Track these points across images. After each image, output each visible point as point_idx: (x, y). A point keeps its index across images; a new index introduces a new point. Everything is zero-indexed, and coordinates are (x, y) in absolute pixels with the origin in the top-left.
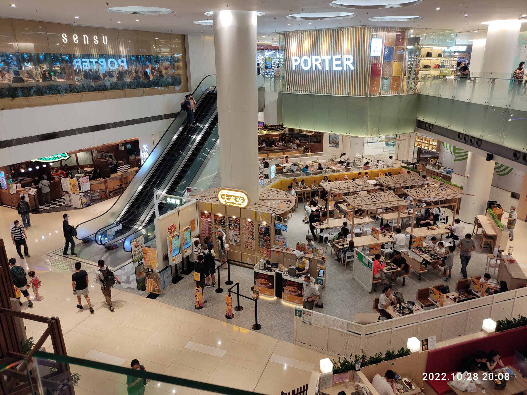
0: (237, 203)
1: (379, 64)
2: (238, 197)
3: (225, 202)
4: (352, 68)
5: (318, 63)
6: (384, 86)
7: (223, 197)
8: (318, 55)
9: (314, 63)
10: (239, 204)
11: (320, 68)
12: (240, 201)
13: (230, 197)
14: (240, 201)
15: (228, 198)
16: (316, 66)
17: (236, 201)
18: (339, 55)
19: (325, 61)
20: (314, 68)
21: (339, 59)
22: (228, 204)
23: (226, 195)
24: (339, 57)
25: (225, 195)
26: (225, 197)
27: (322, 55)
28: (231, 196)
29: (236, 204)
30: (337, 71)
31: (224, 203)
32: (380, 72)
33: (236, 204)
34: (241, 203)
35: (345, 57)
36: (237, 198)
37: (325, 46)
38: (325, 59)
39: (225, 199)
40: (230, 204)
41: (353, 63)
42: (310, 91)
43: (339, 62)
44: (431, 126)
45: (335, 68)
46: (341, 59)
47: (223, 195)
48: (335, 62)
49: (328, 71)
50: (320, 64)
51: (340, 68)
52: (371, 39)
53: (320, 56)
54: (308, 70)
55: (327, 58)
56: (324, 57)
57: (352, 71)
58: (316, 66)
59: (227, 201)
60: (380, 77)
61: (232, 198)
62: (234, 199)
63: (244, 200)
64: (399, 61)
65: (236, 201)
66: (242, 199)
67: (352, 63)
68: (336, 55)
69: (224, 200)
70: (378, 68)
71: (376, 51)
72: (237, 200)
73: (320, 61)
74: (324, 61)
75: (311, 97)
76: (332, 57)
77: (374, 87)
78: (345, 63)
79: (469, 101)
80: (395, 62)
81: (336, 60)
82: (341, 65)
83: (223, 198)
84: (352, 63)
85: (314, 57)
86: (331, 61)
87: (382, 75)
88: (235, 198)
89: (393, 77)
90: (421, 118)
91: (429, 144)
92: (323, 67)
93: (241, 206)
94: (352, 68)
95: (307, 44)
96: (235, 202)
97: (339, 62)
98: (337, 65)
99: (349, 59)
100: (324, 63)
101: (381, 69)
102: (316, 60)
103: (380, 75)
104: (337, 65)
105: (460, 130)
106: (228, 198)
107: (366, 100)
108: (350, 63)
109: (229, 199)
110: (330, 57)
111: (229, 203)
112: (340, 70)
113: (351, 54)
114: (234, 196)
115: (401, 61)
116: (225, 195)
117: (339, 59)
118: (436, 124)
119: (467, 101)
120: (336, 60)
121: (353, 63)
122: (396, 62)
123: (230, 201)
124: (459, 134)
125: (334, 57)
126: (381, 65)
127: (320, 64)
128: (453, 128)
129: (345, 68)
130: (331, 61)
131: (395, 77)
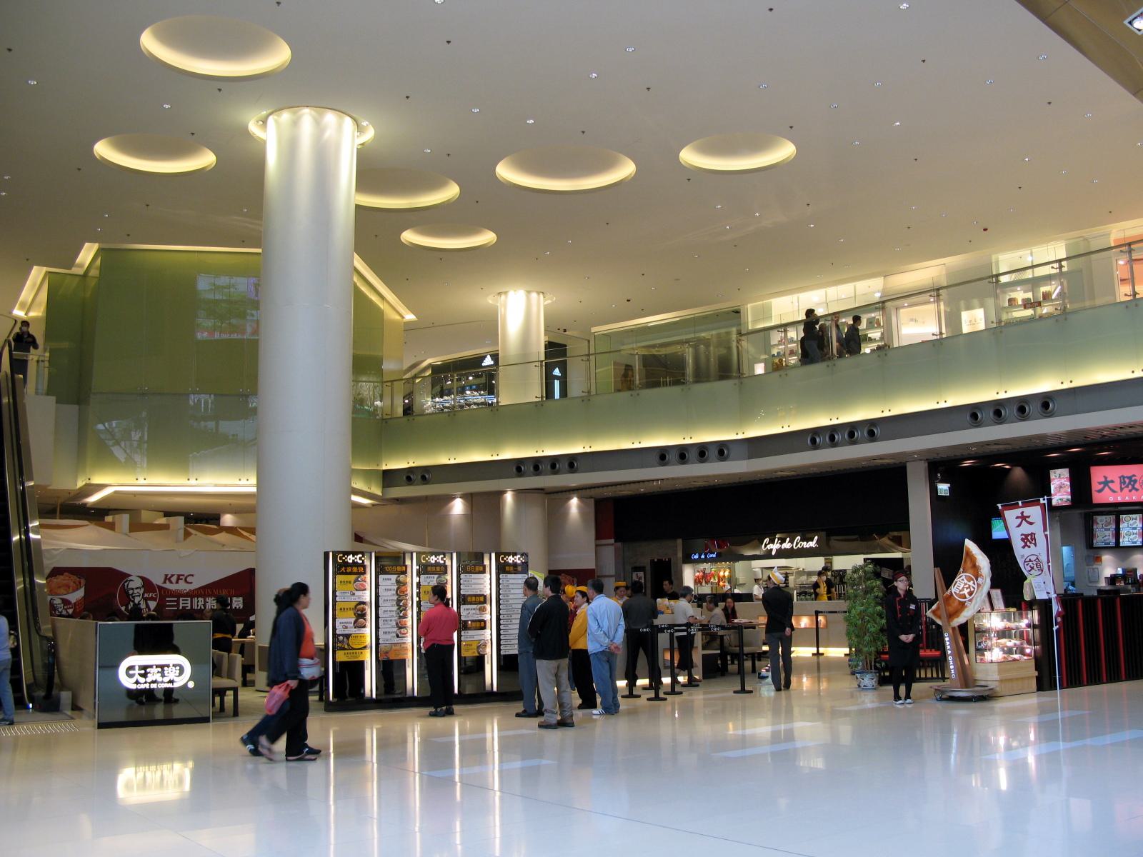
0: (166, 679)
2: (168, 666)
3: (137, 682)
7: (131, 672)
10: (171, 682)
12: (171, 674)
13: (148, 670)
14: (171, 674)
15: (143, 672)
17: (163, 676)
22: (142, 687)
23: (139, 666)
25: (137, 668)
26: (137, 671)
28: (151, 666)
29: (162, 682)
31: (134, 687)
33: (162, 682)
34: (176, 679)
36: (166, 668)
39: (137, 677)
40: (147, 686)
47: (131, 668)
59: (142, 680)
61: (154, 670)
62: (158, 672)
63: (182, 671)
65: (163, 676)
66: (178, 668)
69: (134, 680)
72: (166, 672)
83: (131, 676)
88: (160, 670)
93: (176, 685)
96: (160, 679)
106: (143, 672)
109: (145, 675)
111: (146, 683)
114: (157, 666)
116: (137, 668)
123: (149, 679)
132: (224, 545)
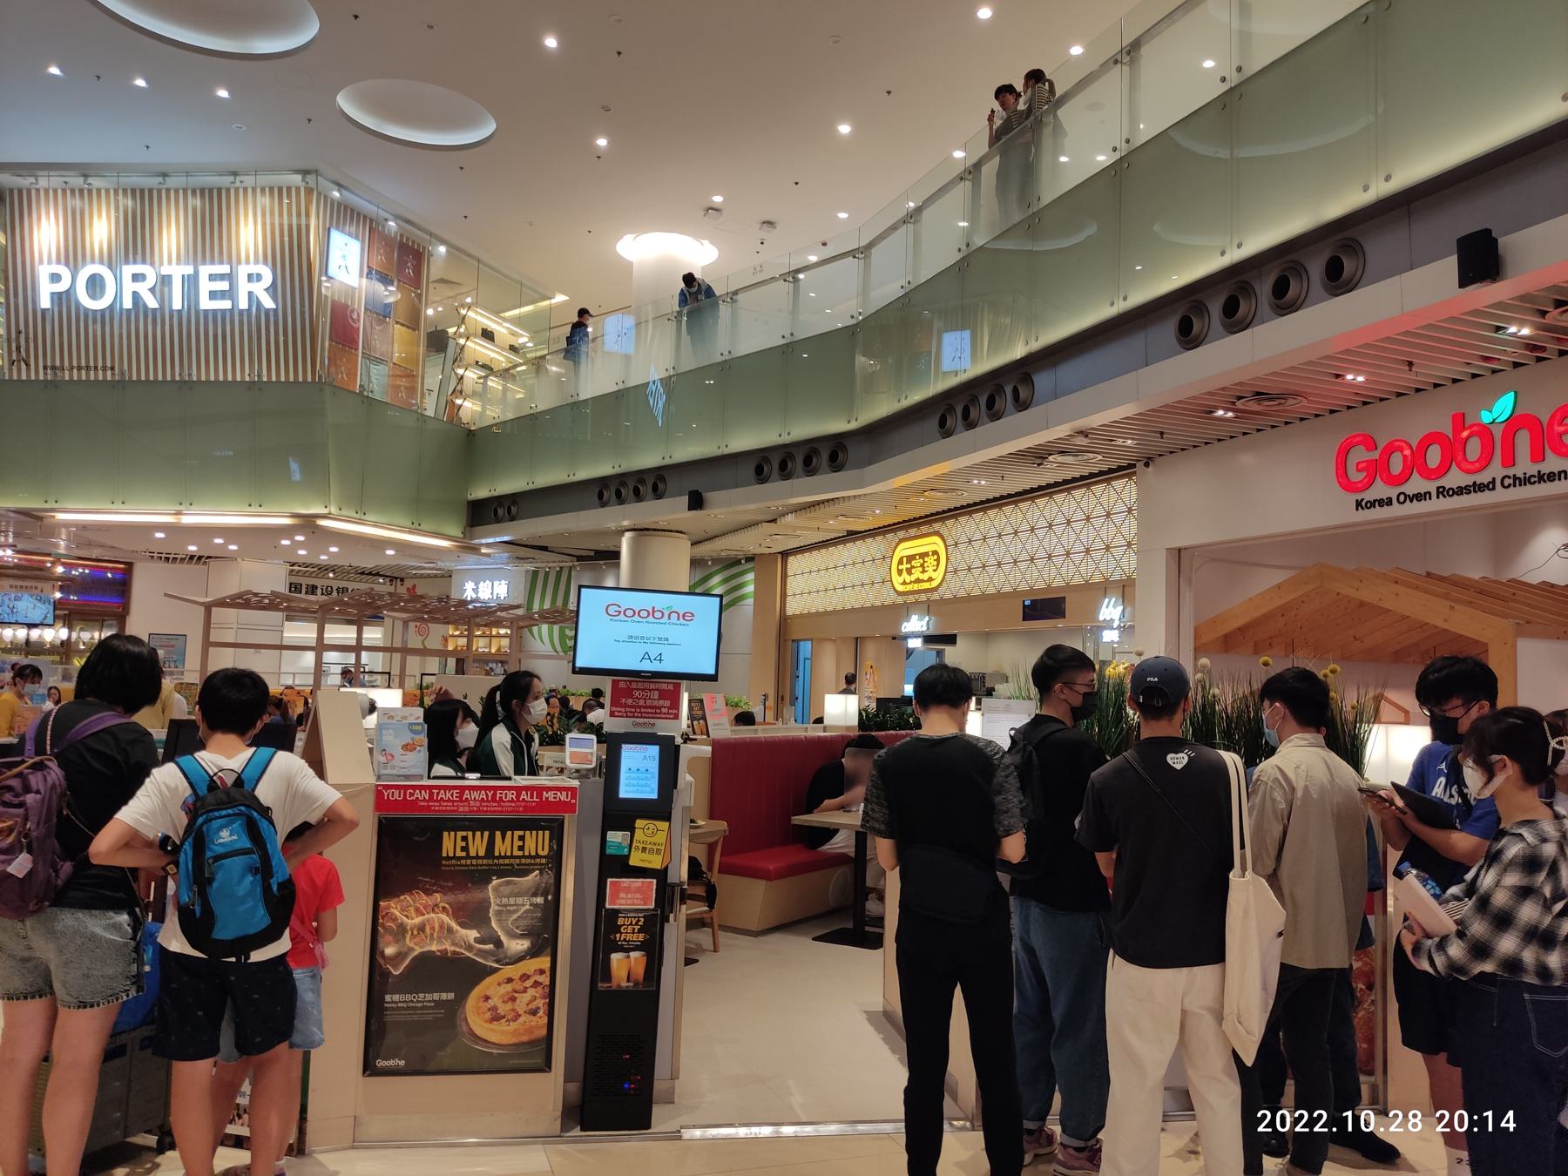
1: (352, 311)
4: (268, 303)
5: (143, 289)
6: (372, 382)
8: (144, 262)
9: (129, 287)
11: (152, 303)
16: (136, 295)
18: (221, 263)
19: (170, 283)
20: (128, 304)
21: (222, 277)
24: (225, 269)
27: (161, 263)
30: (215, 311)
32: (358, 335)
35: (243, 271)
37: (171, 236)
38: (170, 277)
41: (272, 290)
42: (104, 368)
43: (224, 286)
44: (512, 508)
45: (206, 304)
46: (230, 277)
48: (205, 286)
49: (179, 312)
50: (152, 290)
51: (226, 304)
52: (329, 228)
53: (152, 264)
54: (103, 311)
55: (178, 272)
56: (165, 270)
57: (267, 311)
58: (136, 295)
60: (357, 349)
64: (408, 327)
67: (266, 290)
68: (212, 262)
70: (353, 324)
71: (343, 268)
73: (151, 280)
74: (165, 280)
75: (114, 387)
76: (196, 273)
77: (342, 373)
78: (244, 288)
79: (621, 386)
80: (397, 323)
81: (212, 277)
82: (230, 294)
84: (266, 290)
85: (128, 270)
86: (191, 282)
87: (363, 347)
89: (394, 364)
90: (481, 492)
91: (491, 636)
92: (164, 299)
94: (268, 303)
95: (102, 229)
97: (224, 286)
98: (213, 295)
99: (259, 277)
100: (166, 289)
101: (358, 328)
102: (137, 278)
103: (357, 343)
104: (213, 295)
105: (604, 468)
107: (321, 390)
108: (260, 290)
110: (189, 270)
112: (224, 311)
113: (265, 262)
115: (414, 330)
117: (222, 277)
118: (531, 487)
119: (615, 388)
120: (212, 277)
121: (271, 290)
122: (402, 325)
124: (603, 482)
125: (205, 270)
126: (359, 315)
127: (152, 290)
128: (583, 474)
129: (243, 304)
130: (191, 282)
131: (399, 366)
132: (165, 175)
